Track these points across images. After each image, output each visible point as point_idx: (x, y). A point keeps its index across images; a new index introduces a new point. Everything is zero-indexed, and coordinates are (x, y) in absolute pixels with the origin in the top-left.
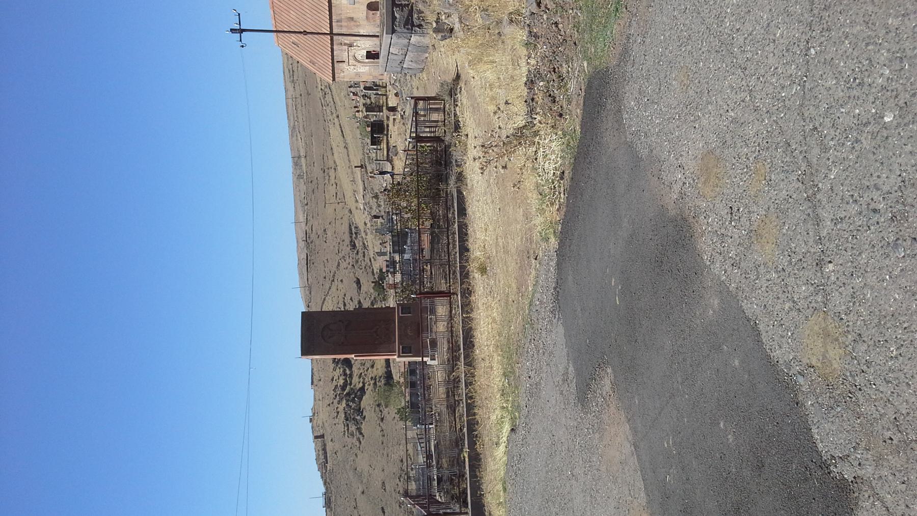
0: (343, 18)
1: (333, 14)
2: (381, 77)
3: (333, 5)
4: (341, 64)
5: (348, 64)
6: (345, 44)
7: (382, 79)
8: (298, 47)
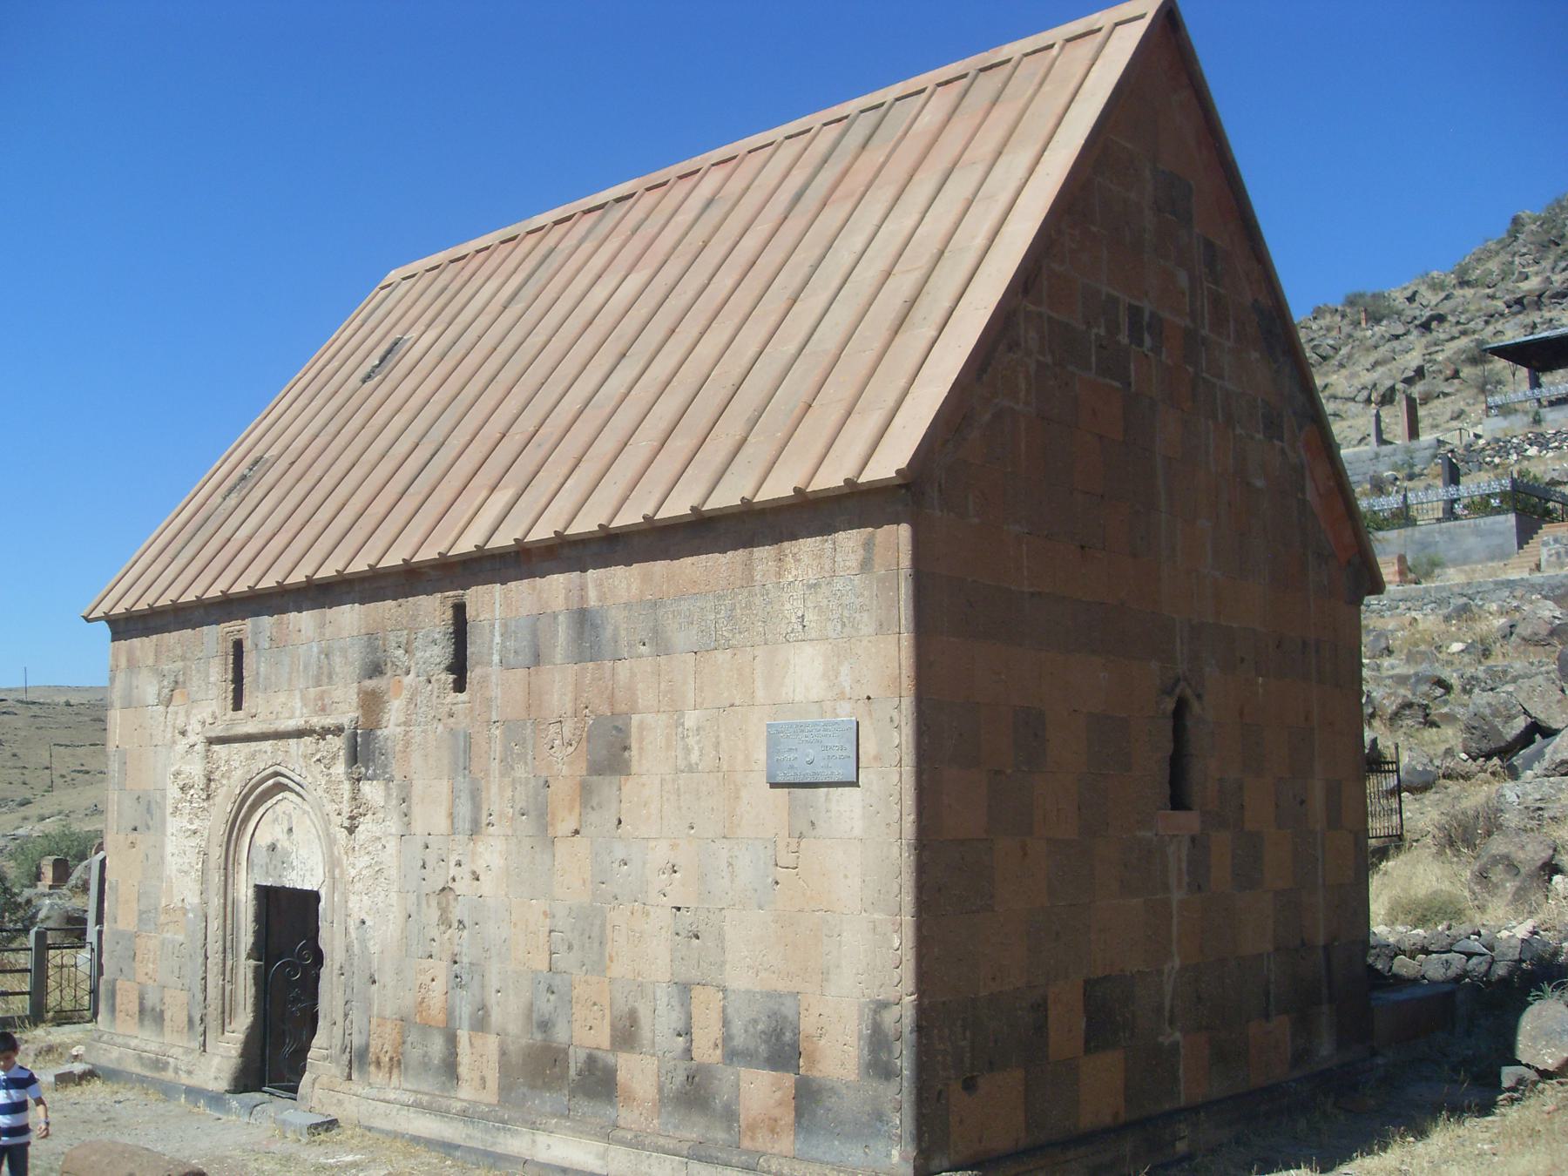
0: (623, 668)
1: (660, 567)
2: (127, 999)
3: (763, 553)
4: (217, 673)
5: (218, 731)
6: (372, 704)
7: (113, 1009)
8: (368, 377)
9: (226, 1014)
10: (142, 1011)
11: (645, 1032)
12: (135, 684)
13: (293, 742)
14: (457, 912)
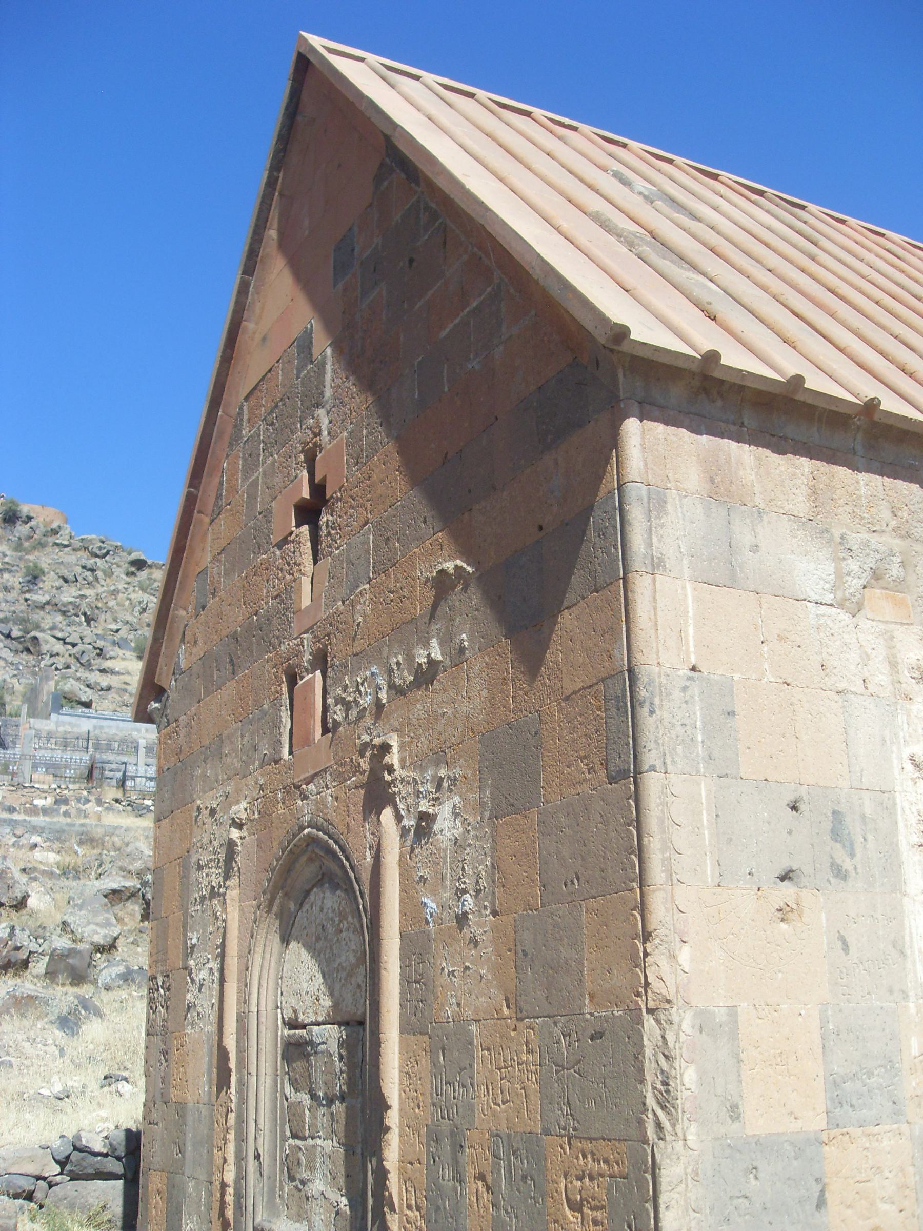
12: (744, 537)
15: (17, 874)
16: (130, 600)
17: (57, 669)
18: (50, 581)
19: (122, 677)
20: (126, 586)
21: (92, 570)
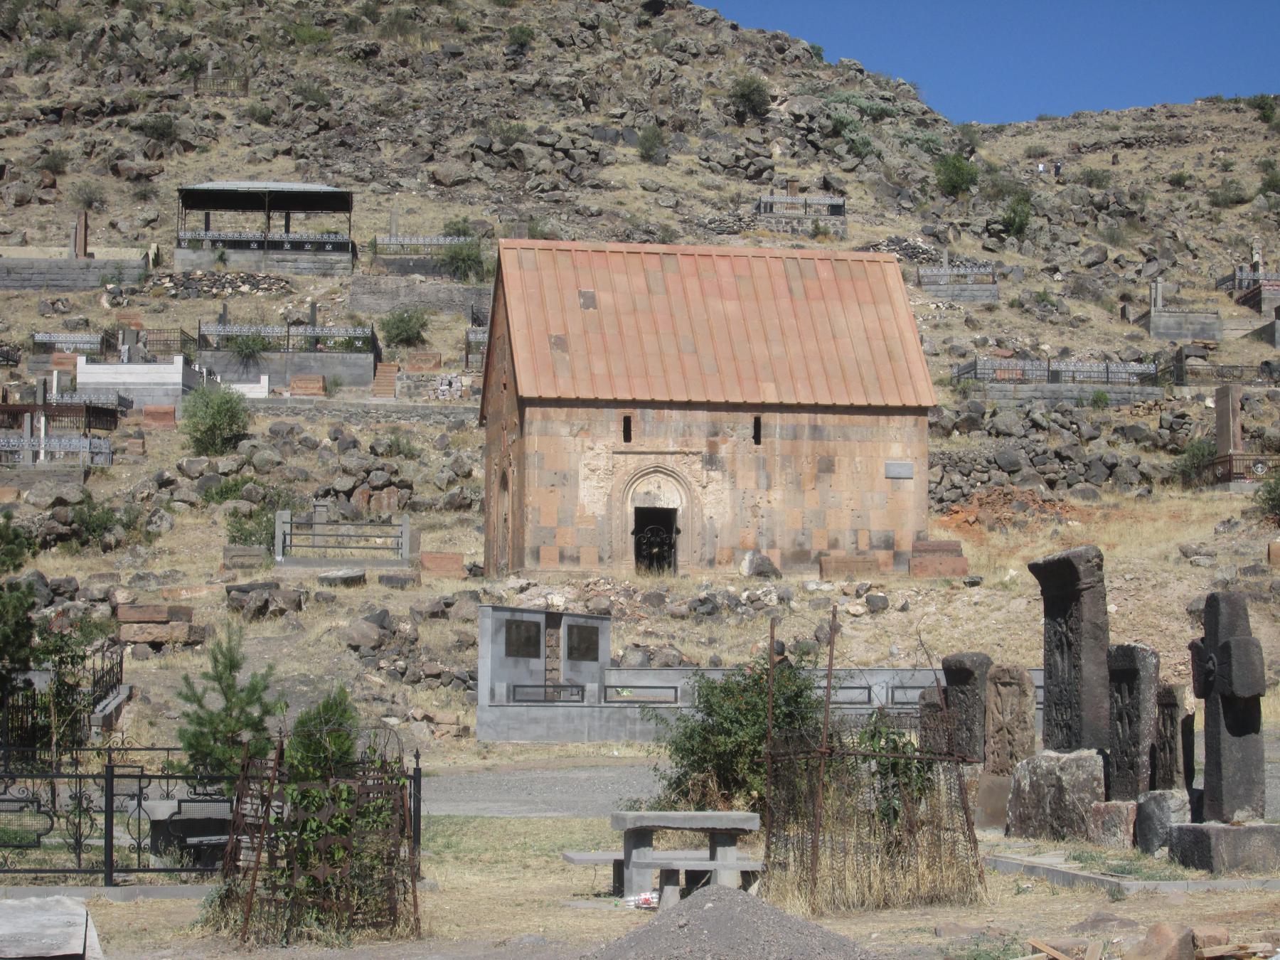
0: (832, 444)
1: (846, 417)
3: (882, 419)
4: (617, 428)
6: (713, 447)
9: (625, 553)
10: (562, 557)
11: (841, 543)
12: (549, 425)
13: (668, 457)
14: (761, 512)
15: (465, 459)
16: (640, 68)
17: (543, 191)
18: (542, 47)
19: (617, 193)
20: (635, 46)
21: (592, 28)
